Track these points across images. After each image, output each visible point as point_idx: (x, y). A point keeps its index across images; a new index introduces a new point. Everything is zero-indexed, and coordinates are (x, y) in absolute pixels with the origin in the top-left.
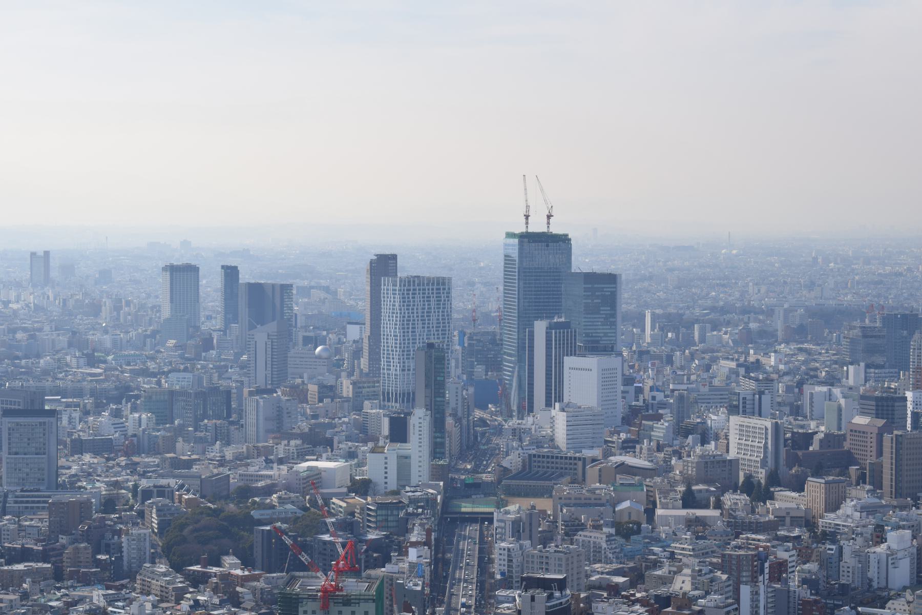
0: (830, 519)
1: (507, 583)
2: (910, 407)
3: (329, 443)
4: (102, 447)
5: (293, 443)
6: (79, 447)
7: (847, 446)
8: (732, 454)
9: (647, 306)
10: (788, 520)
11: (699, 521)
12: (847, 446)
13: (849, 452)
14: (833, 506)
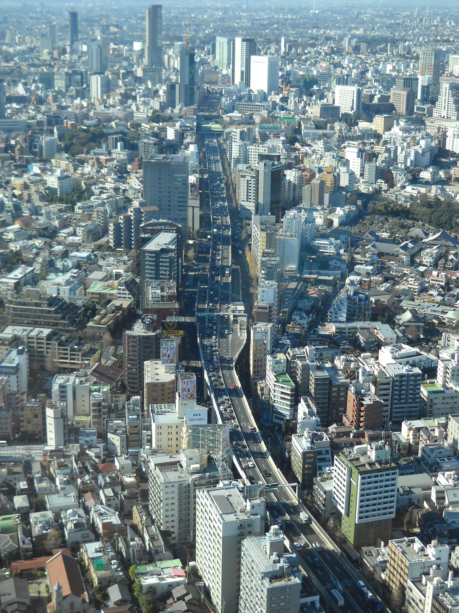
0: (386, 136)
3: (134, 98)
4: (20, 100)
5: (117, 98)
6: (10, 100)
7: (391, 101)
8: (336, 104)
10: (366, 136)
11: (325, 135)
12: (391, 101)
13: (392, 104)
14: (388, 128)
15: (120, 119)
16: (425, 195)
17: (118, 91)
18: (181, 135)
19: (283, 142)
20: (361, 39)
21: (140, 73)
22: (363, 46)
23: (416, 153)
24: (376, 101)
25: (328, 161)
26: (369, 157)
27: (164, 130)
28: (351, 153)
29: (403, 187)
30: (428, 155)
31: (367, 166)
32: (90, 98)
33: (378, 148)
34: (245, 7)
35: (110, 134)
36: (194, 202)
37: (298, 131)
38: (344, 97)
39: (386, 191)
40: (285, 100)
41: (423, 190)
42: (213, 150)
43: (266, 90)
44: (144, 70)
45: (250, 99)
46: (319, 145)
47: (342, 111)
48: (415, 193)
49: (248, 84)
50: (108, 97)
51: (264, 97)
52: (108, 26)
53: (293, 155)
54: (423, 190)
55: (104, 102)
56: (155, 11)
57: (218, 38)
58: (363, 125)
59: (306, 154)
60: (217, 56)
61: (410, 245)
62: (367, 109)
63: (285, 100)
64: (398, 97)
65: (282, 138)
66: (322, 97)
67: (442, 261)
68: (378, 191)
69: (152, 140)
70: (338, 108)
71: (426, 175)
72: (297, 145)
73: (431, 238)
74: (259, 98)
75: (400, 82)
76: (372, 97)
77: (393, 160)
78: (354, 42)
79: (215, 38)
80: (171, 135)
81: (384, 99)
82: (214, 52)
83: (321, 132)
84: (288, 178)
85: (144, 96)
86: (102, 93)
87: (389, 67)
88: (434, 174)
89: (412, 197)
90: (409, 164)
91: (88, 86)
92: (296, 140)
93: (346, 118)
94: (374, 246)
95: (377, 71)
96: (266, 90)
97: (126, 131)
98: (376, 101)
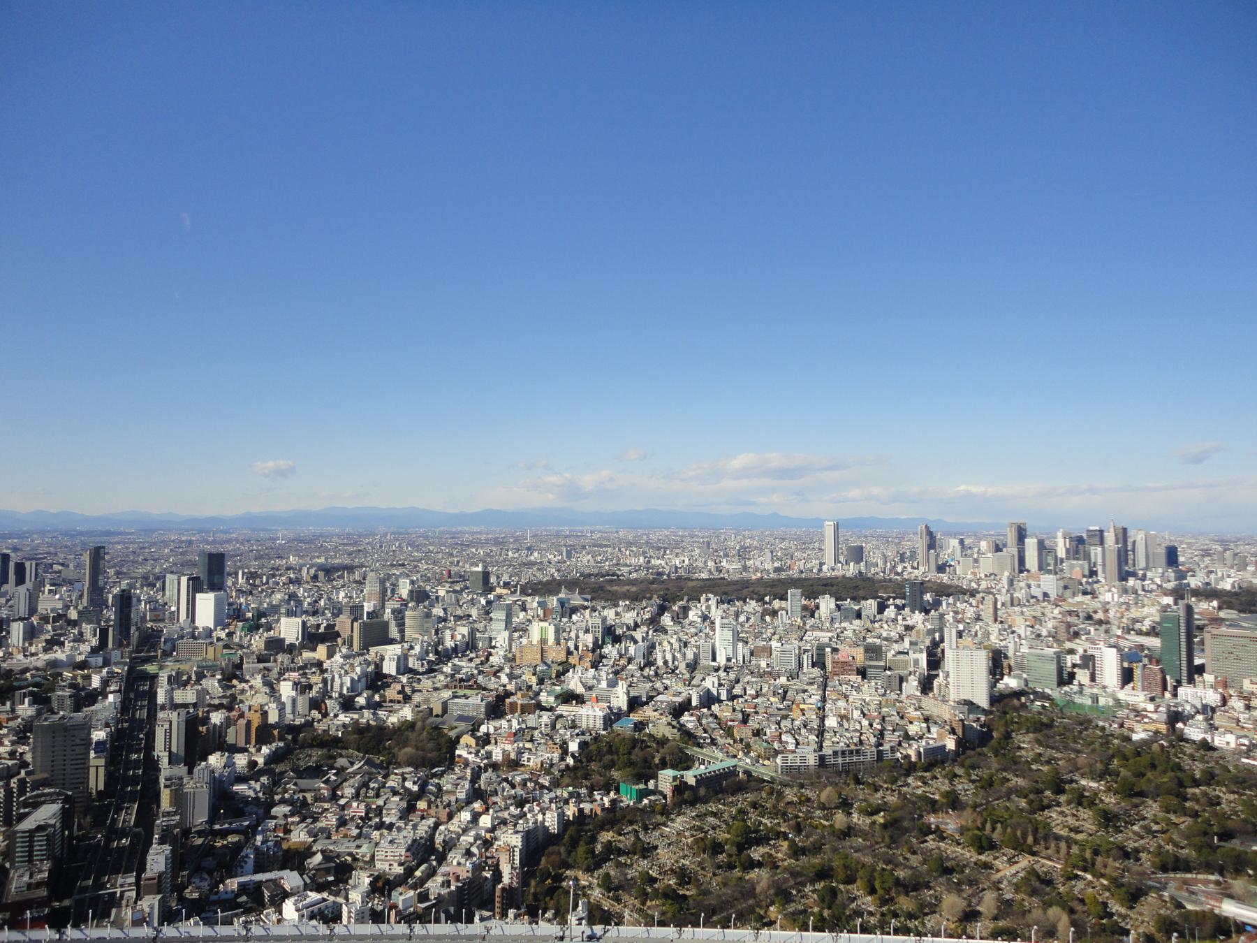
1: (163, 708)
2: (366, 610)
3: (62, 644)
9: (240, 568)
14: (330, 655)
15: (37, 669)
16: (356, 722)
17: (43, 638)
18: (105, 683)
19: (219, 681)
20: (321, 568)
21: (73, 614)
22: (321, 574)
23: (352, 680)
24: (322, 630)
25: (261, 699)
26: (302, 688)
27: (87, 678)
28: (286, 690)
29: (336, 716)
30: (364, 680)
31: (300, 700)
32: (8, 646)
33: (316, 679)
34: (211, 539)
35: (21, 688)
36: (96, 761)
37: (239, 666)
38: (289, 629)
39: (319, 721)
40: (230, 635)
41: (356, 716)
42: (142, 695)
43: (212, 626)
44: (79, 613)
45: (194, 637)
46: (257, 681)
47: (287, 642)
48: (347, 720)
49: (193, 621)
50: (31, 644)
51: (209, 633)
52: (51, 565)
53: (229, 693)
54: (356, 716)
55: (25, 649)
56: (97, 554)
57: (168, 576)
58: (307, 655)
59: (243, 691)
60: (167, 593)
61: (333, 778)
62: (311, 638)
63: (230, 635)
64: (343, 623)
65: (219, 677)
66: (269, 629)
67: (363, 790)
68: (309, 724)
69: (68, 692)
70: (283, 640)
71: (361, 700)
72: (235, 682)
73: (356, 767)
74: (203, 635)
75: (347, 610)
76: (318, 626)
77: (325, 693)
78: (312, 571)
79: (164, 577)
80: (96, 682)
81: (330, 627)
82: (164, 589)
83: (261, 665)
84: (213, 721)
85: (74, 641)
86: (24, 640)
87: (342, 594)
88: (368, 699)
89: (344, 726)
90: (345, 692)
91: (8, 633)
92: (236, 677)
93: (291, 649)
94: (295, 784)
95: (329, 599)
96: (212, 626)
97: (43, 682)
98: (322, 630)
